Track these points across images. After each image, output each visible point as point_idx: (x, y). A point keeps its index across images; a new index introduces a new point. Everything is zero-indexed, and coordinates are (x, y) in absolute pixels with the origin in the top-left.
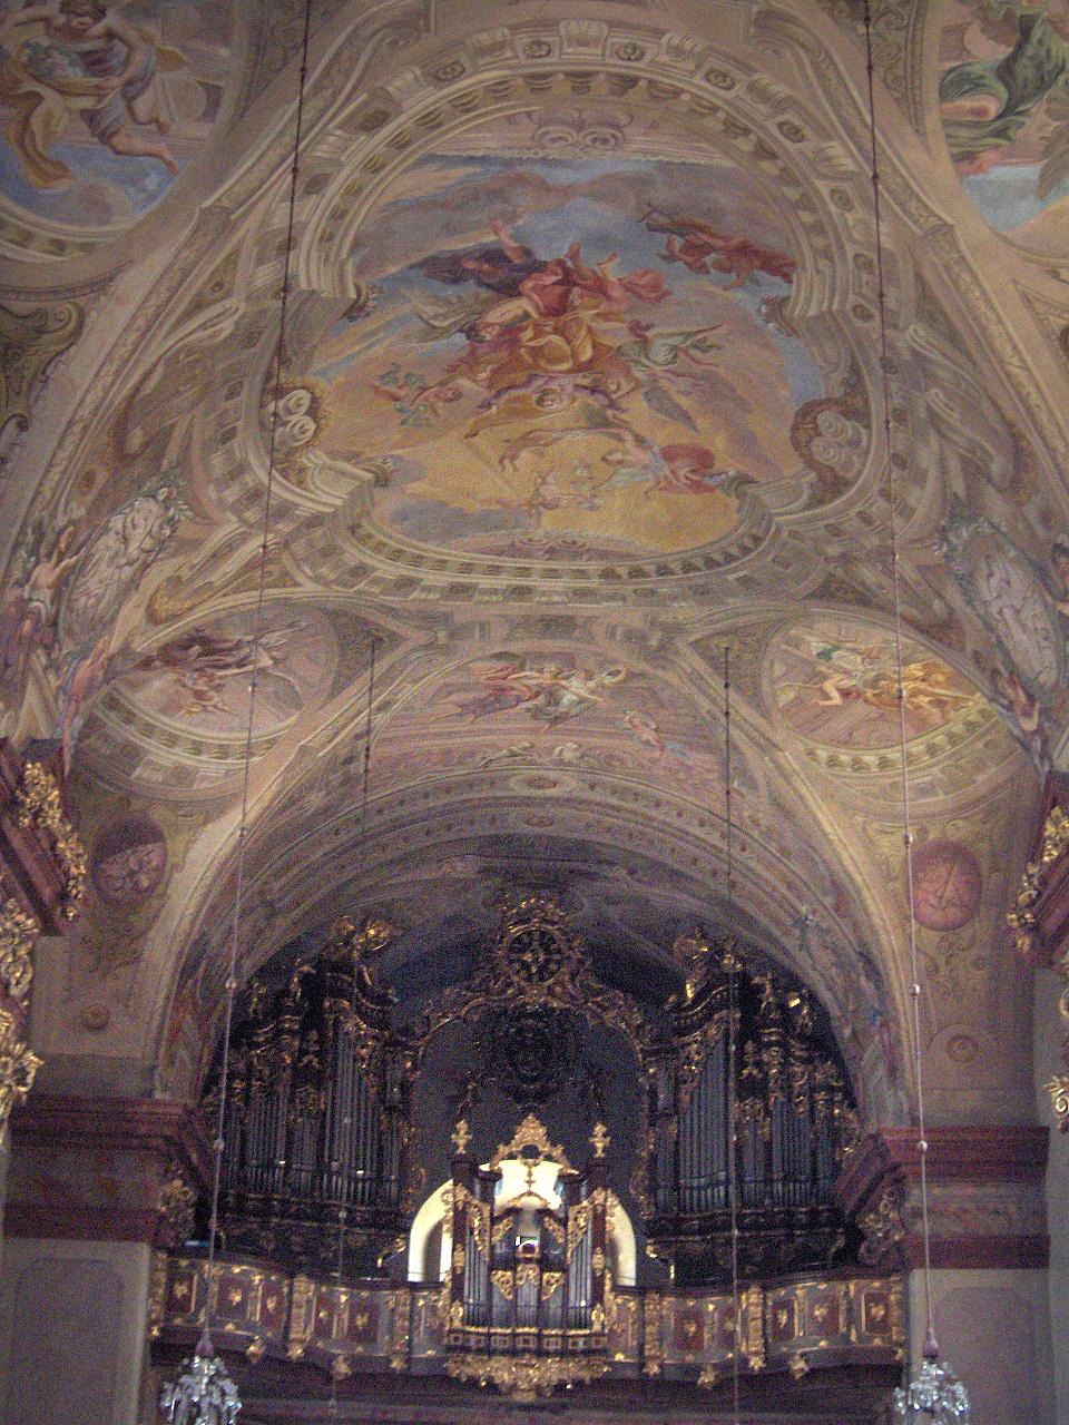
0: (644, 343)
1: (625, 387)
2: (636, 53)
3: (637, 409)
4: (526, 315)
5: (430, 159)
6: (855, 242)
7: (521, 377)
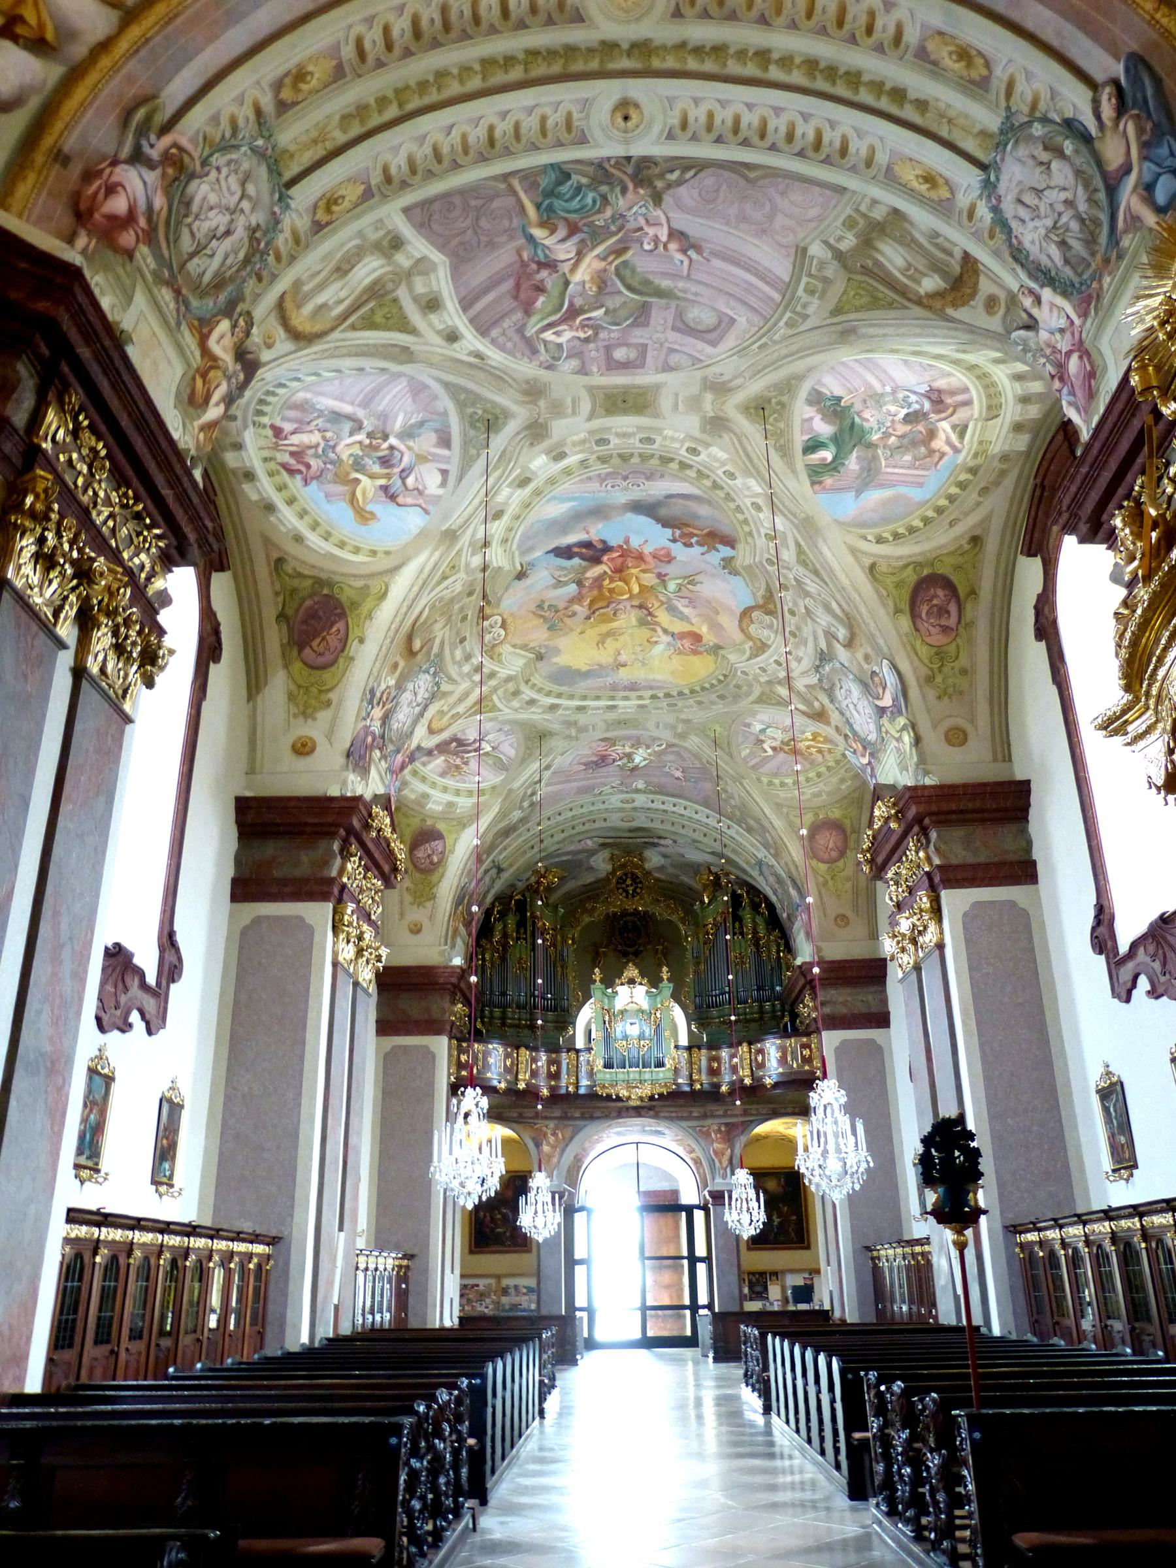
0: (664, 583)
2: (649, 441)
3: (663, 617)
5: (554, 498)
7: (604, 603)
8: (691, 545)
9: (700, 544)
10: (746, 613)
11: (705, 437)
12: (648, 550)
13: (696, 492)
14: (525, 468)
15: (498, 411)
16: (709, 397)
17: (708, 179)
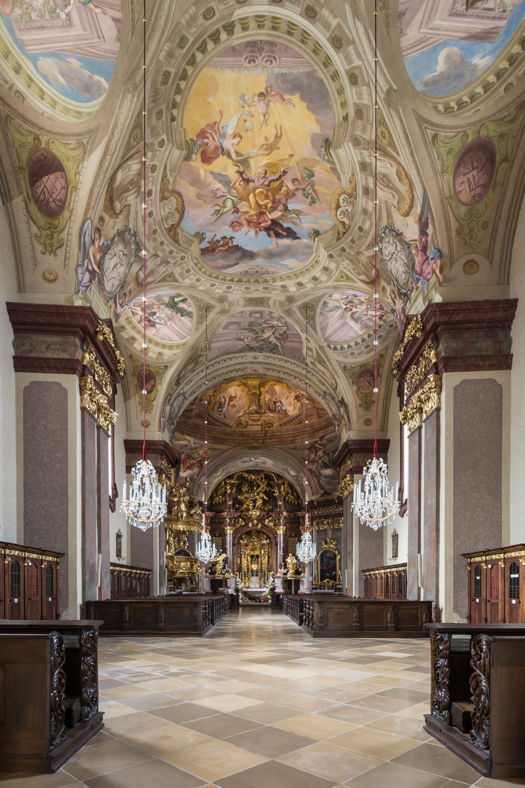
1: (237, 184)
2: (247, 288)
4: (270, 213)
6: (193, 274)
8: (224, 238)
9: (218, 241)
10: (182, 212)
11: (225, 294)
12: (245, 229)
13: (225, 271)
14: (298, 290)
15: (302, 310)
16: (227, 308)
17: (235, 349)
